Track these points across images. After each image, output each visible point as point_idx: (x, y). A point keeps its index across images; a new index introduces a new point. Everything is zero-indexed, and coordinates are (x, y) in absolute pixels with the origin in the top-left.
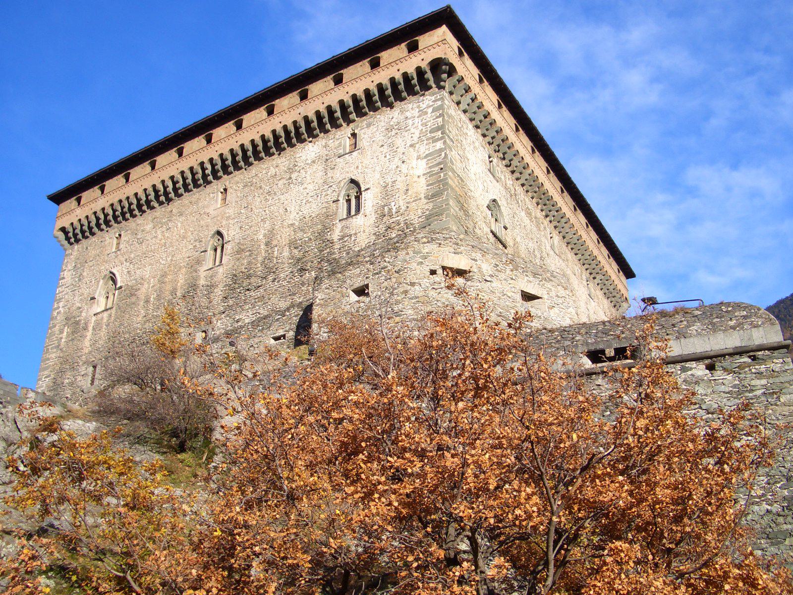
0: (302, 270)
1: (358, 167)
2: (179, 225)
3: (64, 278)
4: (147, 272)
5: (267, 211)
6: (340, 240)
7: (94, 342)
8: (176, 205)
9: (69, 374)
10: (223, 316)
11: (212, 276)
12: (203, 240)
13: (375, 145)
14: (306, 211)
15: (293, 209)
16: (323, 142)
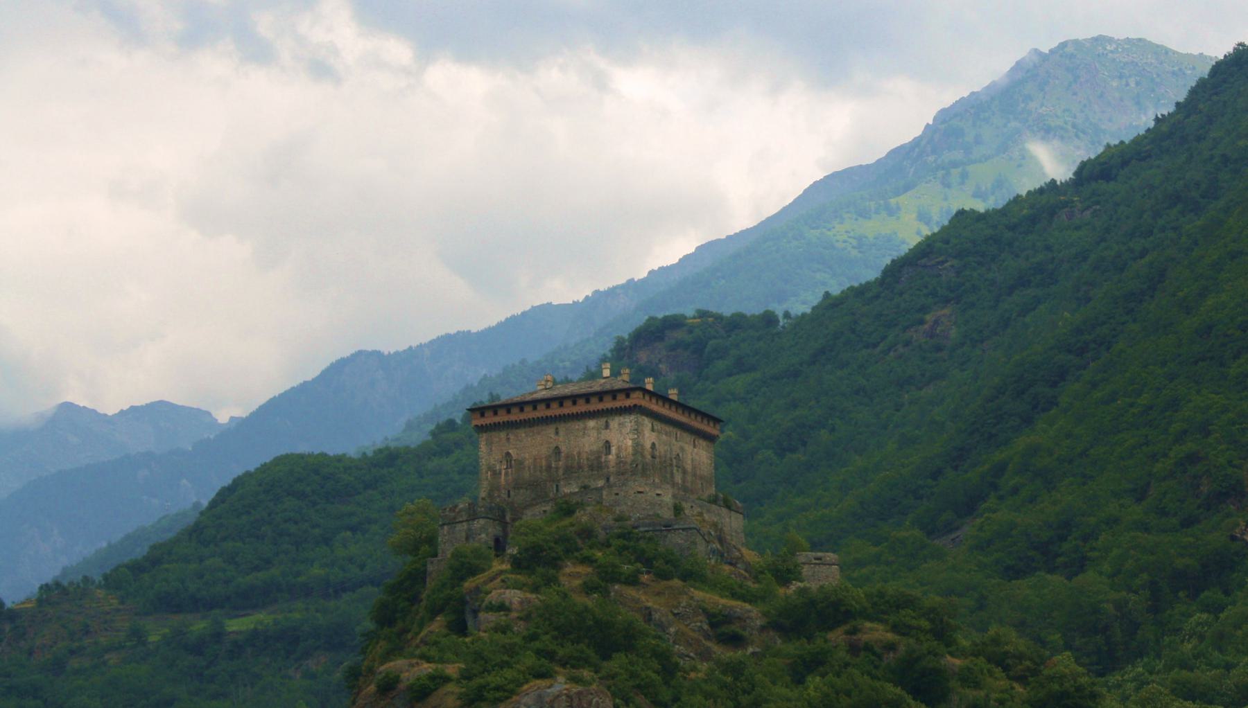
0: (592, 470)
4: (527, 456)
8: (535, 429)
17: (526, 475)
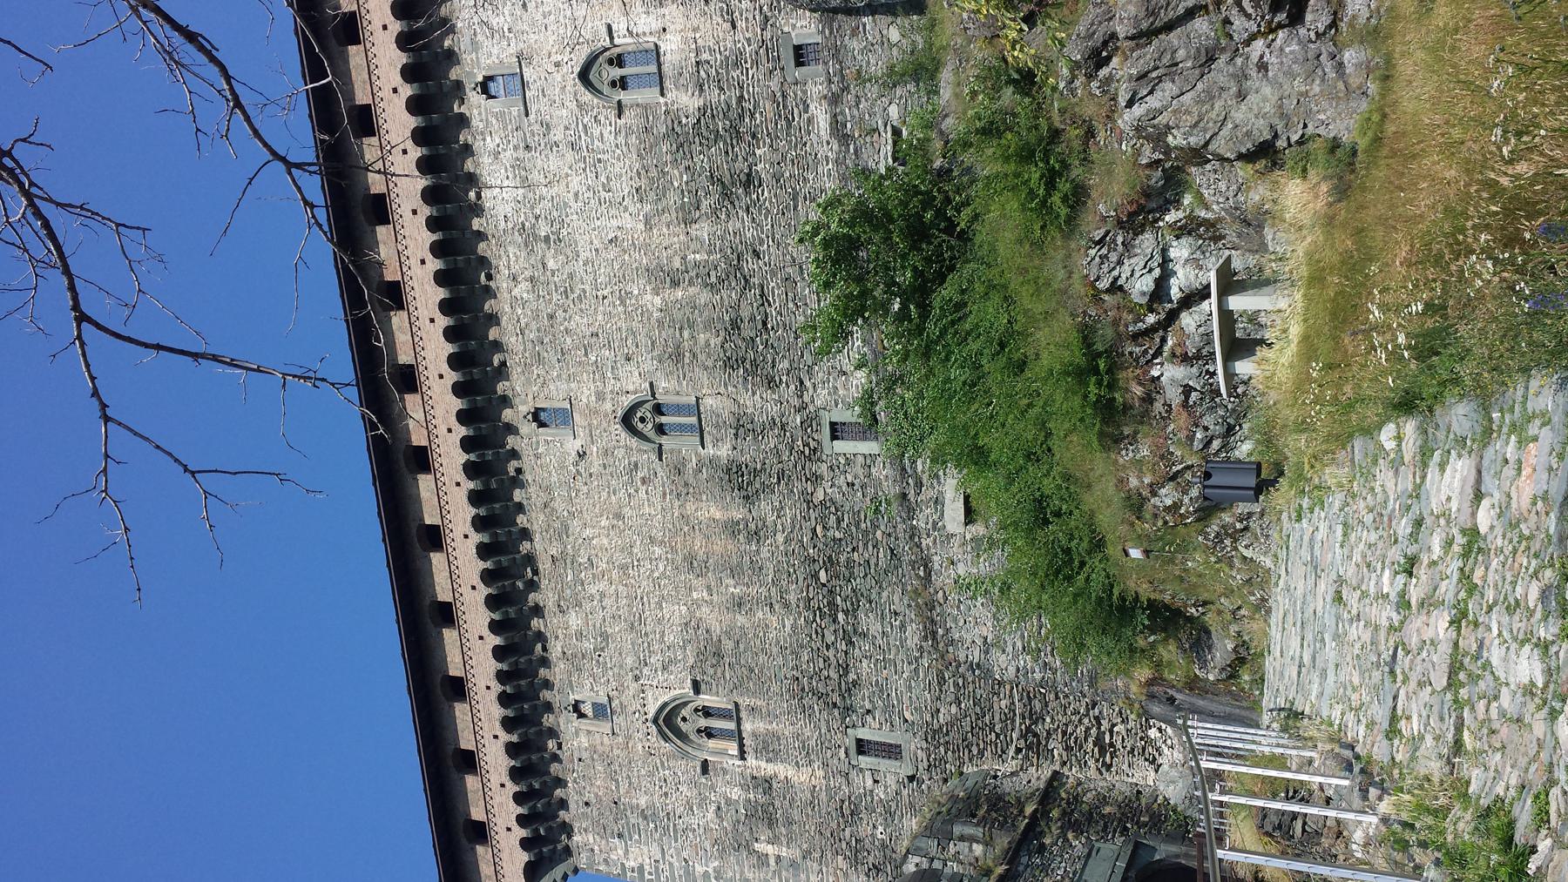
0: (750, 181)
1: (557, 65)
2: (588, 532)
3: (641, 868)
4: (676, 612)
5: (605, 293)
6: (701, 90)
7: (807, 753)
8: (542, 547)
9: (864, 830)
10: (808, 384)
11: (717, 426)
12: (633, 459)
13: (520, 26)
14: (624, 187)
15: (614, 223)
16: (486, 160)
17: (780, 626)
